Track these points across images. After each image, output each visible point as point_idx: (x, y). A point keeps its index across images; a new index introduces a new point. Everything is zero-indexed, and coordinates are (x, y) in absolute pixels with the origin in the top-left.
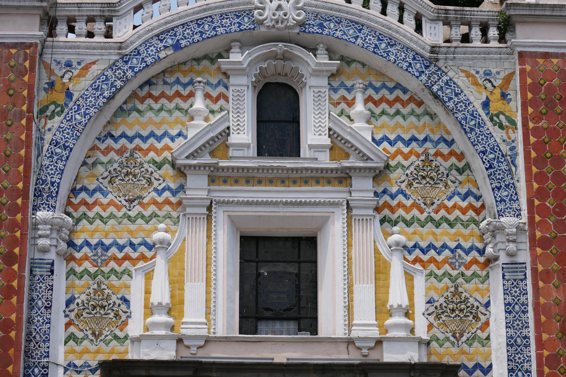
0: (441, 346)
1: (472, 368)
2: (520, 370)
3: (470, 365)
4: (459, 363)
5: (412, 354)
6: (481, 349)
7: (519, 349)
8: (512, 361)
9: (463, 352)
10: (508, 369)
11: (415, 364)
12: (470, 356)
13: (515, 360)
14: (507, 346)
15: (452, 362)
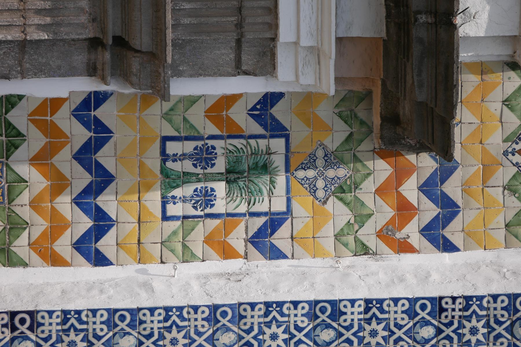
0: (507, 102)
1: (444, 195)
2: (439, 331)
3: (452, 188)
4: (457, 153)
5: (483, 18)
6: (500, 221)
7: (500, 330)
8: (466, 308)
9: (488, 169)
10: (441, 298)
11: (453, 28)
12: (477, 187)
13: (468, 319)
14: (508, 296)
15: (459, 134)
